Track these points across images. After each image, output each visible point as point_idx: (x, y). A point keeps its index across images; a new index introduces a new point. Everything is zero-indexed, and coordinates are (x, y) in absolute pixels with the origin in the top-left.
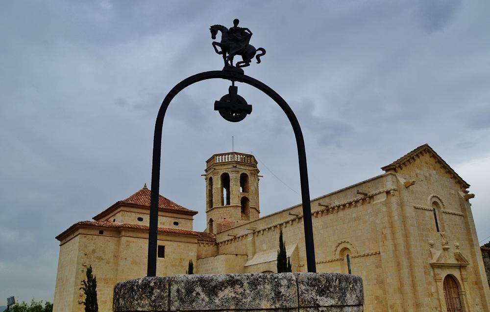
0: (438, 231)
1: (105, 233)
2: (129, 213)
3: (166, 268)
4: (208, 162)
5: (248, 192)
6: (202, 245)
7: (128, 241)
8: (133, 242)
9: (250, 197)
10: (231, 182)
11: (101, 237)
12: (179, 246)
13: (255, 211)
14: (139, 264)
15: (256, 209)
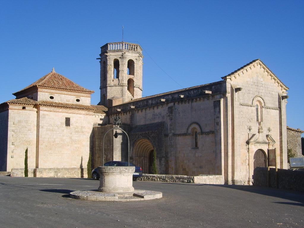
0: (258, 120)
1: (27, 108)
2: (43, 93)
3: (71, 134)
4: (101, 48)
5: (133, 74)
6: (97, 116)
7: (44, 115)
8: (47, 115)
9: (135, 80)
10: (120, 67)
11: (24, 111)
12: (81, 117)
13: (139, 90)
14: (52, 130)
15: (139, 88)
